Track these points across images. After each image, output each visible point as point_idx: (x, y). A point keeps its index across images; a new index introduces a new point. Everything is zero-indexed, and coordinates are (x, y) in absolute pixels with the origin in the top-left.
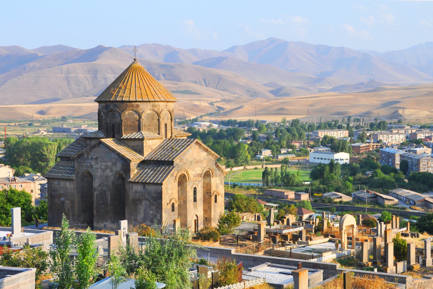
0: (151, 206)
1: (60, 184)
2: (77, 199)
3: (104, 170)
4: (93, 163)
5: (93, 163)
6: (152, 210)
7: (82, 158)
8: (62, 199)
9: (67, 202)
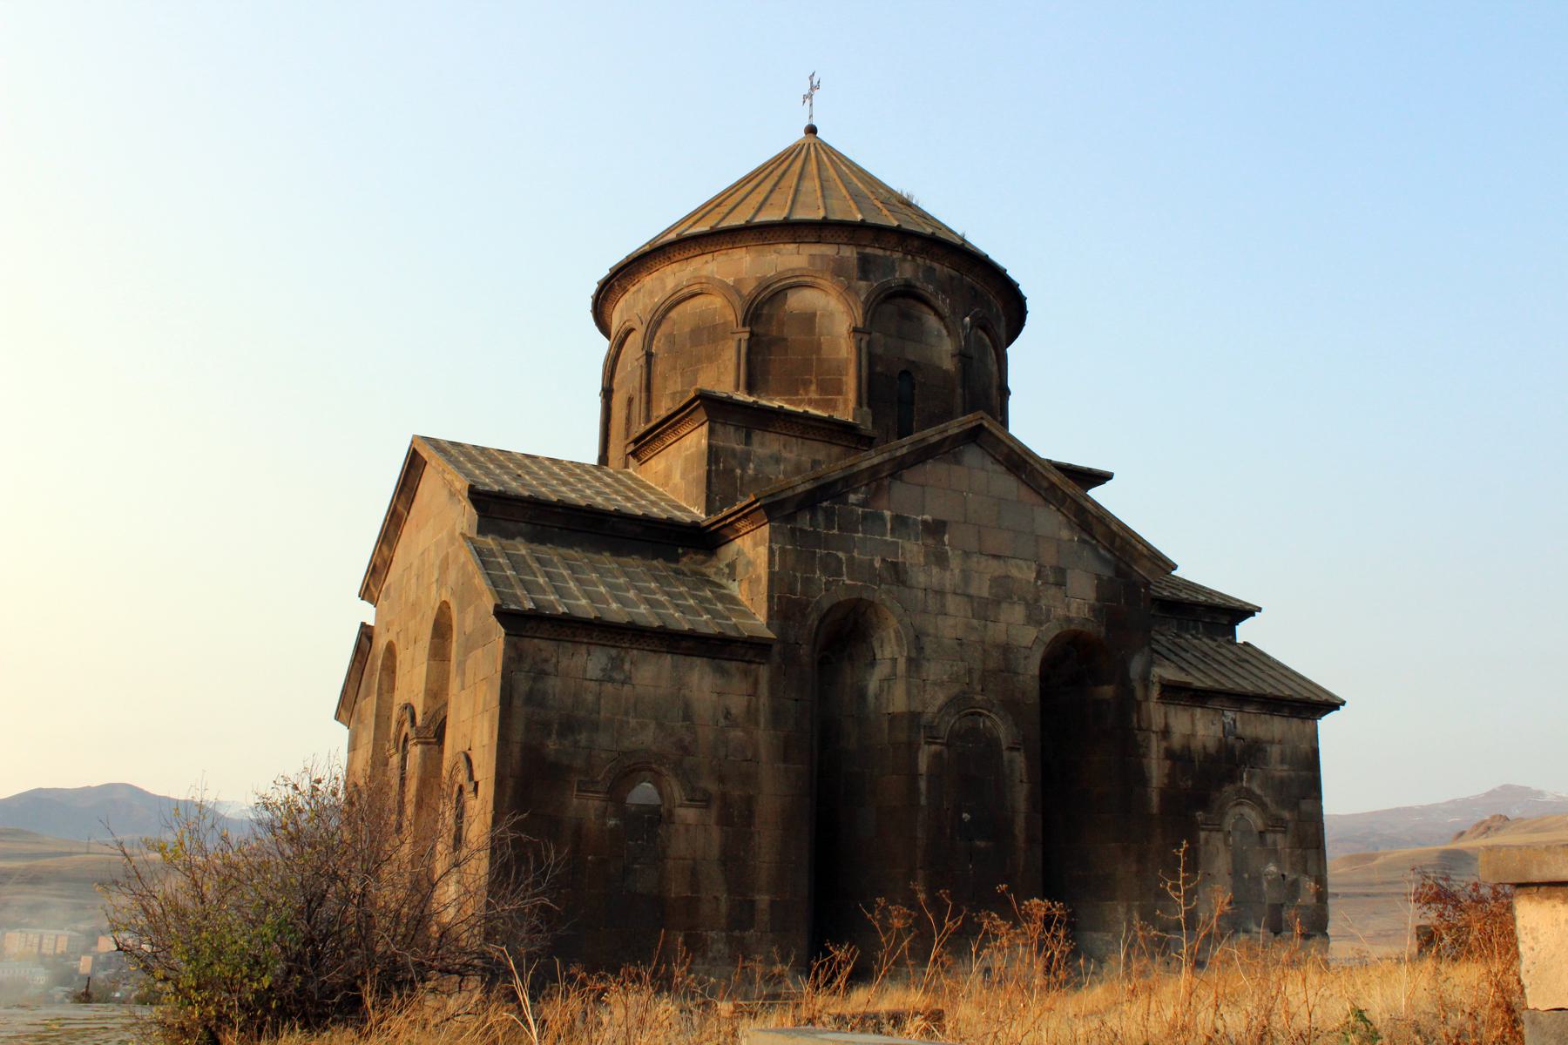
0: (1269, 837)
1: (627, 680)
2: (773, 791)
3: (984, 609)
4: (912, 551)
5: (912, 551)
6: (1274, 854)
7: (829, 514)
8: (643, 793)
9: (689, 814)
